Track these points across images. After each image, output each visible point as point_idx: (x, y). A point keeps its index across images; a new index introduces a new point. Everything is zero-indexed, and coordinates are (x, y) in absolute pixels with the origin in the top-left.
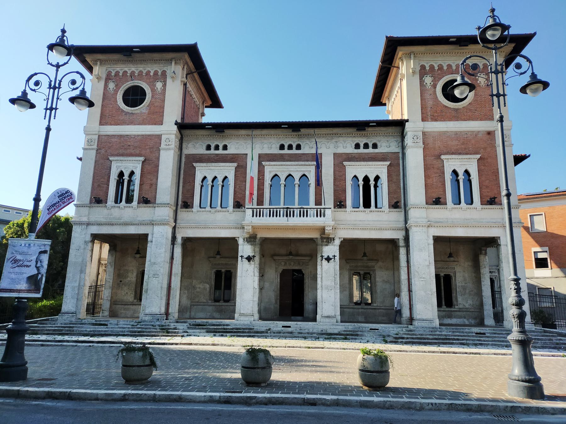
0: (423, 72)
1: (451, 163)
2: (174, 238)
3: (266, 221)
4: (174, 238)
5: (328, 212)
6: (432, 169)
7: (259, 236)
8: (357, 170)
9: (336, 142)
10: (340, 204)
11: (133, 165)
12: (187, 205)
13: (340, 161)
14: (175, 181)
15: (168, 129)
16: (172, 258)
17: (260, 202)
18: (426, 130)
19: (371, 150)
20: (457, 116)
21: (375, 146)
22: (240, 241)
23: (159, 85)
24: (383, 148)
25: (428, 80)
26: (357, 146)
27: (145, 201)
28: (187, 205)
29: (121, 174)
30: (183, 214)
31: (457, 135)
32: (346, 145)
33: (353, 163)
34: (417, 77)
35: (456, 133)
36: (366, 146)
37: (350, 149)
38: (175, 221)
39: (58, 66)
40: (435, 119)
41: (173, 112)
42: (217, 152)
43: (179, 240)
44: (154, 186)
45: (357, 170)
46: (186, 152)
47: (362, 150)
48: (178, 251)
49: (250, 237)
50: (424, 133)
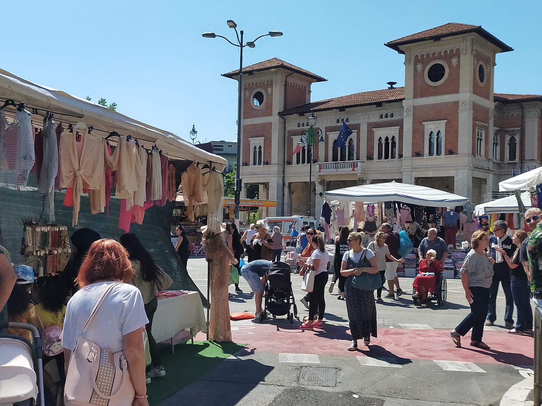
0: (417, 61)
1: (430, 127)
2: (284, 184)
3: (332, 171)
4: (284, 184)
5: (359, 164)
6: (418, 131)
7: (326, 180)
8: (381, 133)
9: (369, 115)
10: (370, 157)
11: (258, 142)
12: (290, 163)
13: (372, 126)
14: (282, 148)
15: (274, 119)
16: (284, 195)
17: (326, 160)
18: (415, 105)
19: (389, 119)
20: (436, 92)
21: (392, 116)
22: (317, 184)
23: (269, 90)
24: (396, 118)
25: (419, 67)
26: (381, 117)
27: (267, 163)
28: (290, 163)
29: (255, 148)
30: (288, 168)
31: (435, 106)
32: (374, 116)
33: (378, 129)
34: (412, 64)
35: (434, 105)
36: (387, 116)
37: (377, 119)
38: (284, 174)
39: (193, 139)
40: (422, 96)
41: (278, 105)
42: (303, 128)
43: (287, 184)
44: (270, 153)
45: (381, 133)
46: (288, 129)
47: (384, 119)
48: (286, 190)
49: (321, 181)
50: (414, 107)
